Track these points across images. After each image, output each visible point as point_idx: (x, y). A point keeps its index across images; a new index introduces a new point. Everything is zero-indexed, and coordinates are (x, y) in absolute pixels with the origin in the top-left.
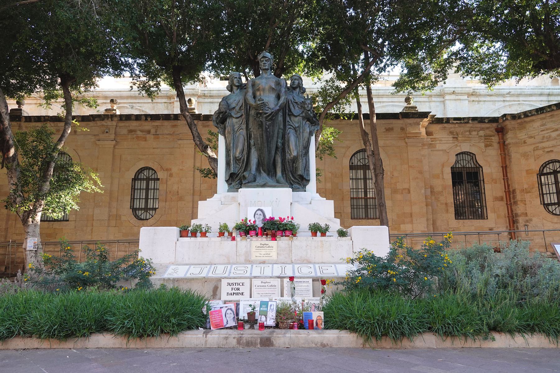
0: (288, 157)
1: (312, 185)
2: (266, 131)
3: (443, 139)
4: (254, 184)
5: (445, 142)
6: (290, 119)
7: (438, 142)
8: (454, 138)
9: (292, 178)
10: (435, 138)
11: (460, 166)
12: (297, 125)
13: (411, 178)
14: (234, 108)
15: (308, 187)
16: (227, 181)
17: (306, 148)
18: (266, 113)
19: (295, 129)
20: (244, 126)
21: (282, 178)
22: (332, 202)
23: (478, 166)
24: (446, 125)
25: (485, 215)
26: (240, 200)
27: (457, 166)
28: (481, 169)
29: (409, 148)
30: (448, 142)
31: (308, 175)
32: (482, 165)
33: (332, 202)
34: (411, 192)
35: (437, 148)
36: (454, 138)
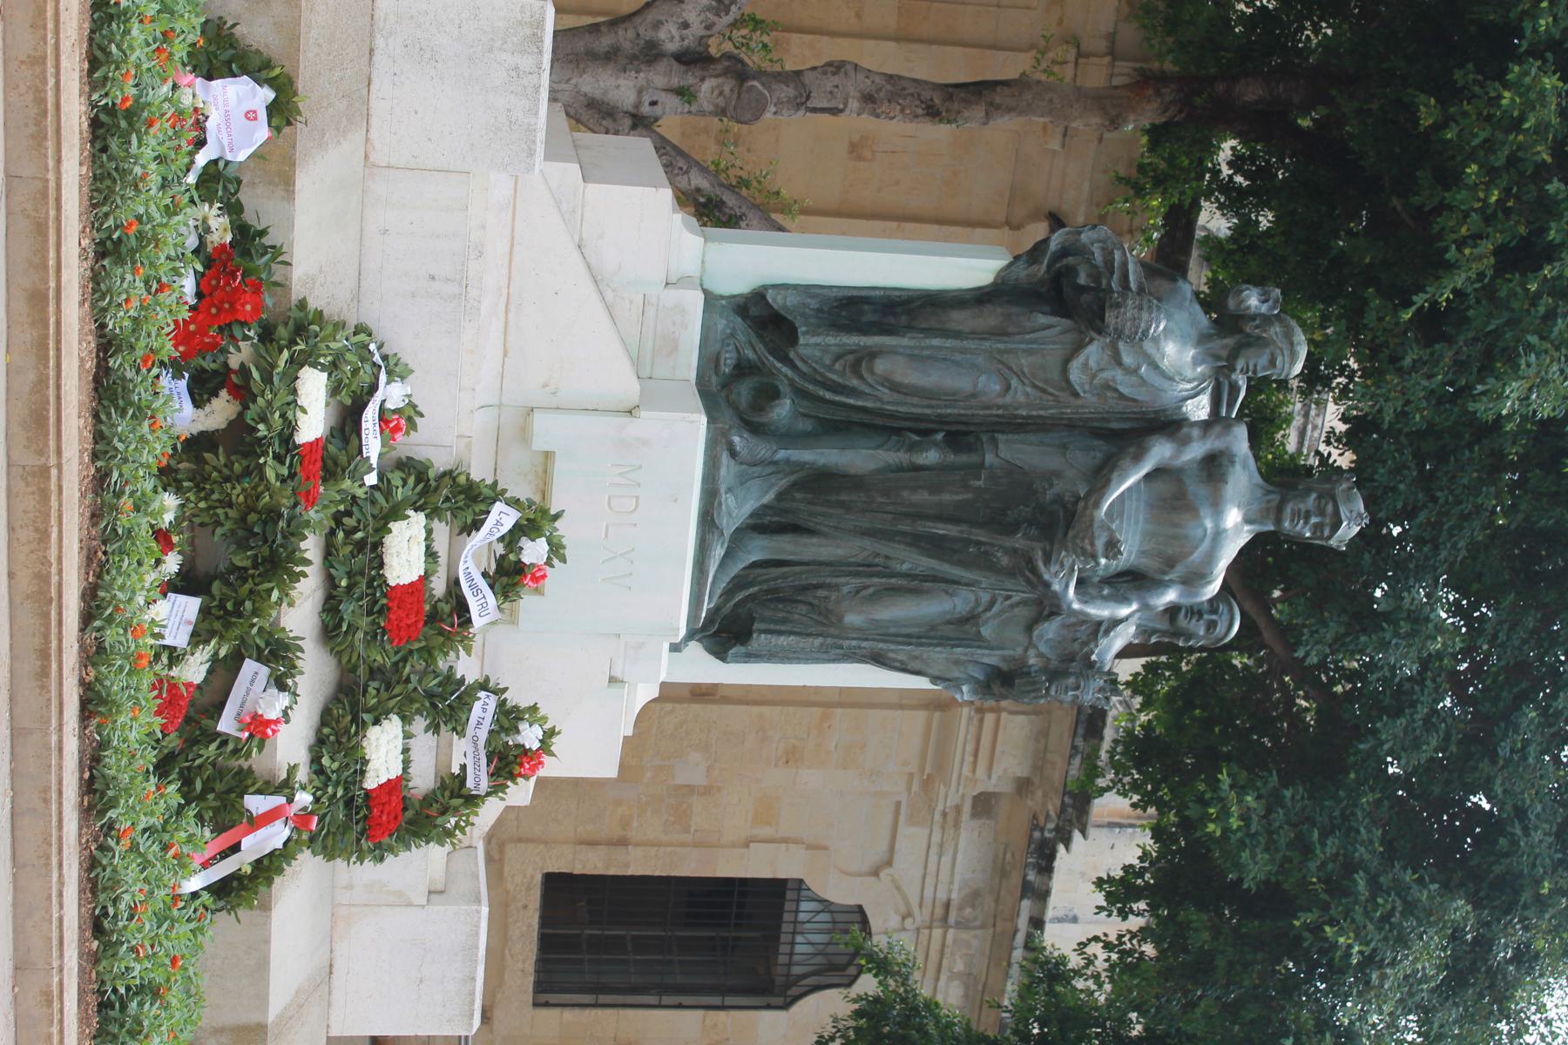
0: (849, 584)
1: (701, 667)
2: (968, 542)
3: (946, 860)
4: (728, 470)
5: (932, 867)
6: (1024, 603)
7: (936, 838)
8: (947, 906)
9: (740, 596)
10: (957, 825)
11: (802, 917)
12: (986, 631)
13: (765, 710)
14: (1118, 362)
15: (695, 649)
16: (758, 295)
17: (878, 659)
18: (1047, 561)
19: (971, 618)
20: (1021, 397)
21: (741, 566)
22: (611, 772)
23: (794, 991)
24: (1015, 880)
25: (553, 998)
26: (650, 422)
27: (804, 906)
28: (779, 1001)
29: (921, 715)
30: (930, 881)
31: (751, 657)
32: (795, 1008)
33: (611, 772)
34: (696, 707)
35: (903, 830)
36: (947, 906)
